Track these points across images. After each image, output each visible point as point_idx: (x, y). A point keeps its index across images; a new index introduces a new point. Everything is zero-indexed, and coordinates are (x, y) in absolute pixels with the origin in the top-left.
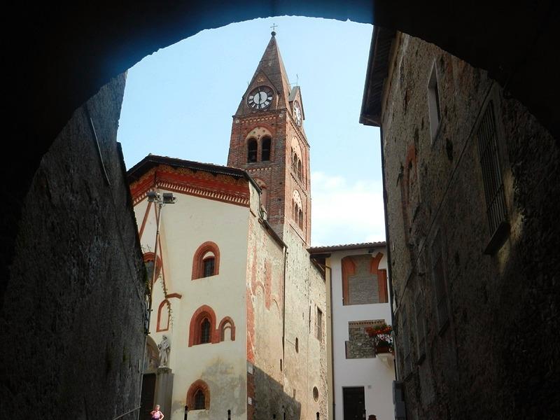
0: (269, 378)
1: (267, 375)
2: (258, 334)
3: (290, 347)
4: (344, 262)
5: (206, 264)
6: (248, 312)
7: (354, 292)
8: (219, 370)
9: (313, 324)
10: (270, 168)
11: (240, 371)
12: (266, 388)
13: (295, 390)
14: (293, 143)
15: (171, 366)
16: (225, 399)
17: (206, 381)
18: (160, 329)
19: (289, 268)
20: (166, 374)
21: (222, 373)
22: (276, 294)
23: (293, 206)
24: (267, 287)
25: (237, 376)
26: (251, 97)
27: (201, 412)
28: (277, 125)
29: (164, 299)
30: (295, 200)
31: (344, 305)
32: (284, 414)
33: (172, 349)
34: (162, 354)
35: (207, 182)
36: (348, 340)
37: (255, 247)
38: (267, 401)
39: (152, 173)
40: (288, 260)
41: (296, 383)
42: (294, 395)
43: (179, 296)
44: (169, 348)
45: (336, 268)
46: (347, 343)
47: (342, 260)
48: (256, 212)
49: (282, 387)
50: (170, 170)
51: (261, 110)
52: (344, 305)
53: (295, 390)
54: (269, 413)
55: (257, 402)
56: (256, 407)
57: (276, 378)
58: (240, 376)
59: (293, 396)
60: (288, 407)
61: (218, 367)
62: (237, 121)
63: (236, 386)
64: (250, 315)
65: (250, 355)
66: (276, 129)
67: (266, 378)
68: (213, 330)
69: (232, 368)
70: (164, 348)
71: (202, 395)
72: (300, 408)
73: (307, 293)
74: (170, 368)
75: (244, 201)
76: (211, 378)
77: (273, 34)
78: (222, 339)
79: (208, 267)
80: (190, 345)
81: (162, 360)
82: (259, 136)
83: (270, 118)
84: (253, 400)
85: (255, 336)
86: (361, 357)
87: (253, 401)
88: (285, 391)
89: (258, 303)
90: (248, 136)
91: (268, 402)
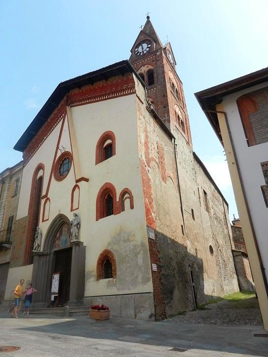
0: (173, 242)
1: (170, 239)
2: (157, 202)
4: (239, 103)
5: (106, 150)
6: (143, 183)
7: (260, 128)
8: (122, 239)
9: (202, 201)
10: (155, 89)
11: (141, 237)
12: (171, 251)
13: (196, 250)
14: (170, 75)
15: (82, 239)
16: (130, 267)
17: (111, 250)
19: (178, 156)
20: (77, 247)
21: (125, 241)
22: (170, 172)
23: (176, 116)
24: (161, 164)
25: (139, 243)
26: (136, 50)
27: (109, 281)
30: (177, 112)
31: (249, 146)
32: (191, 272)
34: (74, 230)
35: (101, 88)
36: (265, 184)
37: (146, 128)
38: (174, 264)
40: (177, 150)
41: (196, 244)
42: (196, 254)
43: (87, 180)
44: (79, 223)
45: (232, 113)
46: (264, 188)
47: (238, 102)
48: (143, 98)
49: (186, 248)
51: (144, 55)
52: (249, 146)
53: (196, 250)
54: (177, 275)
55: (163, 267)
56: (163, 272)
57: (180, 240)
58: (142, 242)
59: (195, 255)
60: (193, 264)
61: (121, 236)
63: (138, 253)
64: (146, 183)
65: (150, 223)
66: (156, 63)
67: (169, 242)
68: (114, 203)
69: (134, 235)
70: (75, 224)
71: (110, 264)
72: (202, 264)
73: (195, 178)
74: (81, 240)
75: (131, 90)
76: (116, 247)
77: (148, 17)
78: (123, 210)
81: (74, 235)
82: (145, 71)
83: (151, 58)
84: (157, 265)
85: (154, 203)
87: (159, 267)
88: (188, 251)
89: (154, 175)
91: (174, 264)
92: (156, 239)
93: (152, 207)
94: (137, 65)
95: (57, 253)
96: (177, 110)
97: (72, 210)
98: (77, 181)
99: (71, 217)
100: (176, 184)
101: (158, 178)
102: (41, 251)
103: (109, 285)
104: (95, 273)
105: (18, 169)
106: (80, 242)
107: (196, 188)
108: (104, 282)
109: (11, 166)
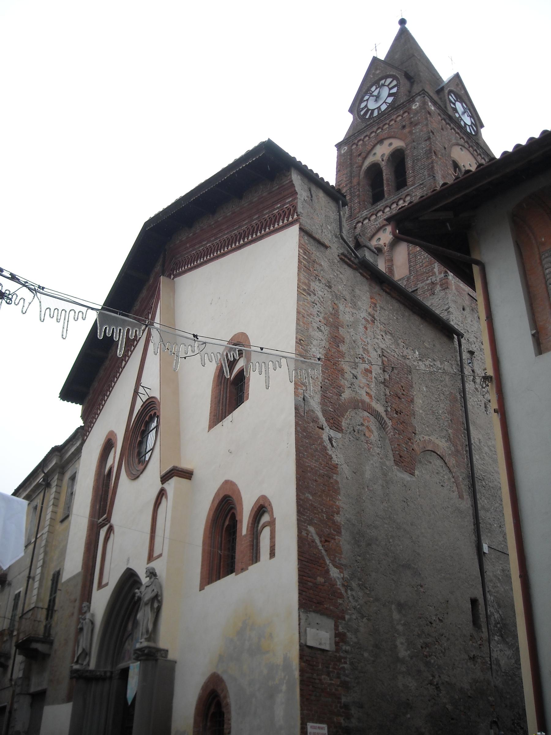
26: (363, 105)
28: (411, 123)
29: (159, 486)
37: (335, 314)
43: (187, 475)
51: (382, 114)
66: (411, 132)
77: (403, 22)
82: (383, 155)
92: (337, 651)
93: (334, 552)
94: (364, 145)
98: (165, 478)
100: (461, 473)
102: (92, 666)
105: (73, 450)
106: (159, 650)
109: (60, 442)
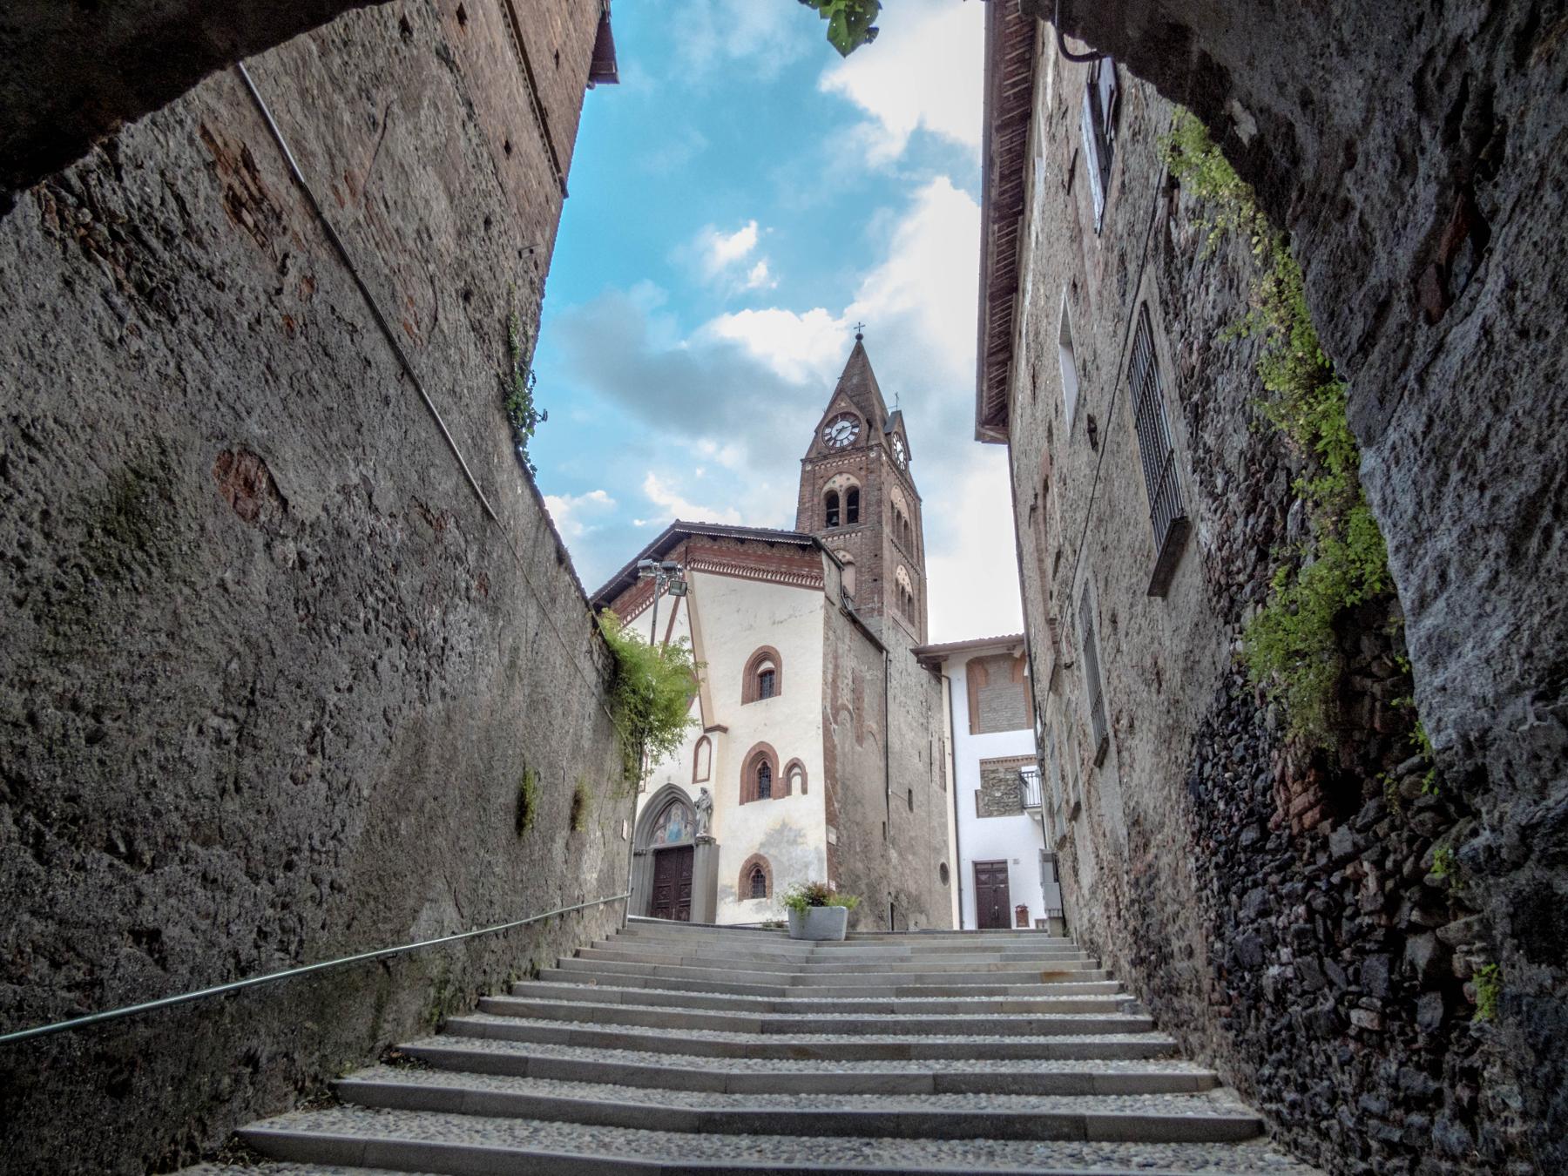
3: (898, 803)
12: (860, 865)
15: (714, 834)
18: (699, 777)
22: (872, 724)
25: (812, 848)
33: (716, 808)
36: (979, 787)
39: (681, 548)
43: (724, 730)
45: (958, 677)
50: (708, 544)
51: (843, 449)
62: (809, 468)
76: (773, 851)
77: (859, 337)
79: (767, 684)
80: (742, 803)
83: (857, 459)
85: (838, 787)
86: (1002, 814)
90: (826, 488)
91: (863, 887)
95: (659, 853)
96: (902, 574)
97: (695, 781)
98: (707, 730)
99: (694, 794)
100: (881, 743)
101: (851, 734)
103: (759, 909)
104: (736, 889)
107: (924, 743)
108: (749, 903)
